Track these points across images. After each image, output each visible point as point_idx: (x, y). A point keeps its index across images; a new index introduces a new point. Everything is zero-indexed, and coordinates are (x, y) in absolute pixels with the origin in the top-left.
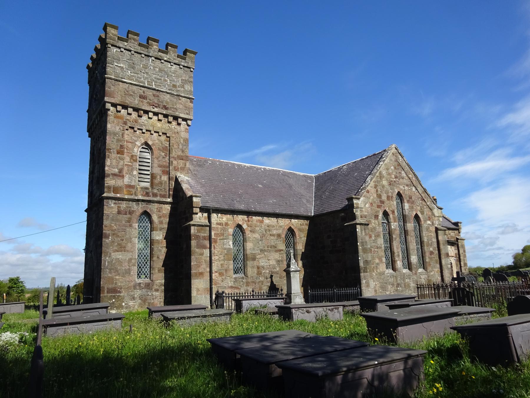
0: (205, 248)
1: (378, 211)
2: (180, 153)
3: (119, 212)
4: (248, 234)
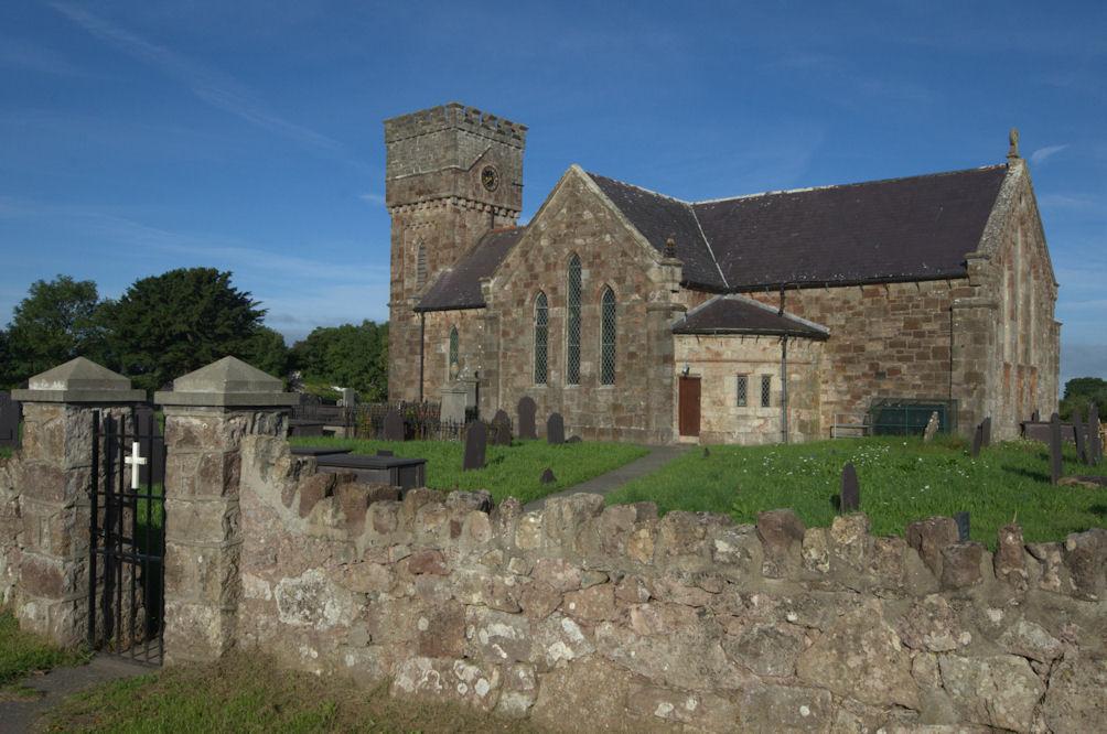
0: (416, 354)
1: (525, 294)
2: (445, 241)
3: (399, 319)
4: (461, 335)
